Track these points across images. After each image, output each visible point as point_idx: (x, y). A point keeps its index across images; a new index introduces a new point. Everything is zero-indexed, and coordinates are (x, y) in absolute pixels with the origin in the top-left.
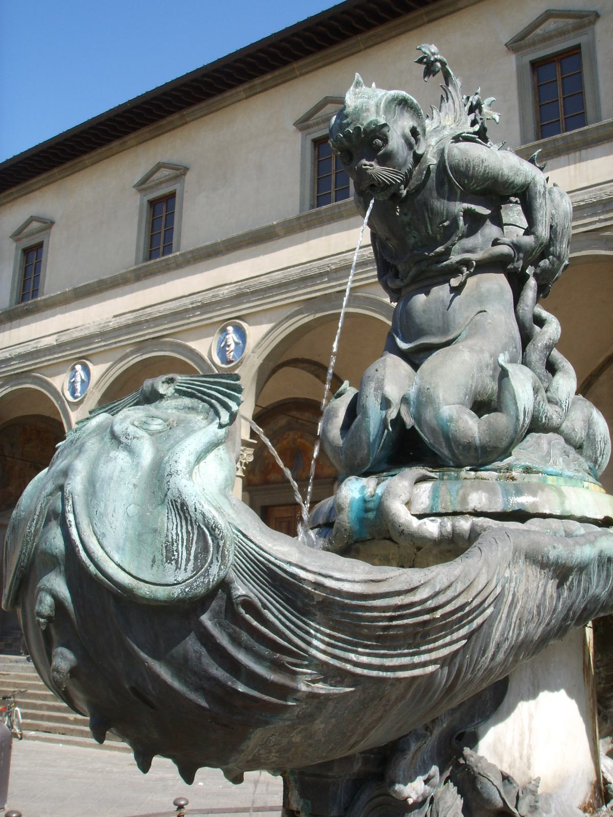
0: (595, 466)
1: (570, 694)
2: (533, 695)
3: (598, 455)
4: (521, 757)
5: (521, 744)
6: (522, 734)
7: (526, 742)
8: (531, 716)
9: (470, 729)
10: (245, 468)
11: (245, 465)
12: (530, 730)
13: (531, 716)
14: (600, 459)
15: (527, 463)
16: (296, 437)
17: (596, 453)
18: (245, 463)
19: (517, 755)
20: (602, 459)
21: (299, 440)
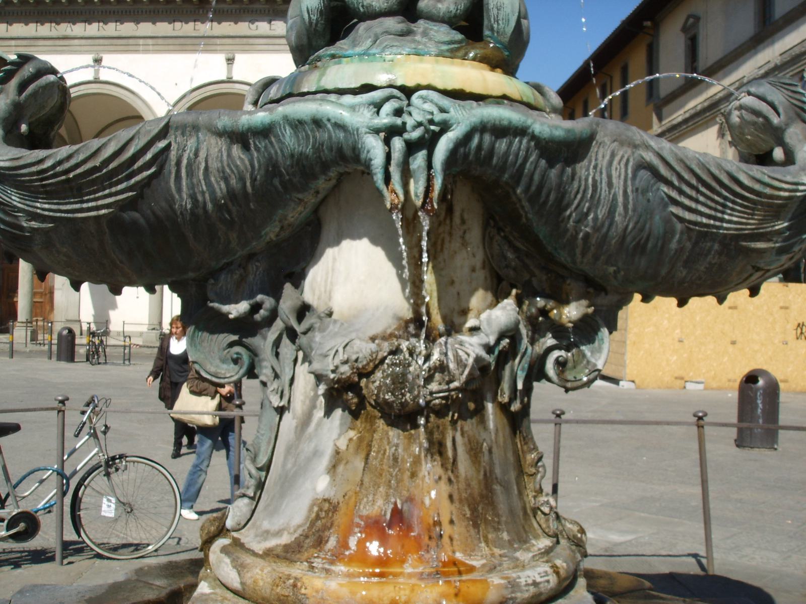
0: (493, 34)
1: (375, 241)
2: (337, 242)
4: (325, 291)
5: (326, 281)
6: (327, 273)
7: (329, 280)
8: (334, 259)
9: (297, 269)
12: (333, 270)
13: (334, 259)
14: (495, 26)
15: (332, 52)
19: (323, 289)
20: (498, 24)
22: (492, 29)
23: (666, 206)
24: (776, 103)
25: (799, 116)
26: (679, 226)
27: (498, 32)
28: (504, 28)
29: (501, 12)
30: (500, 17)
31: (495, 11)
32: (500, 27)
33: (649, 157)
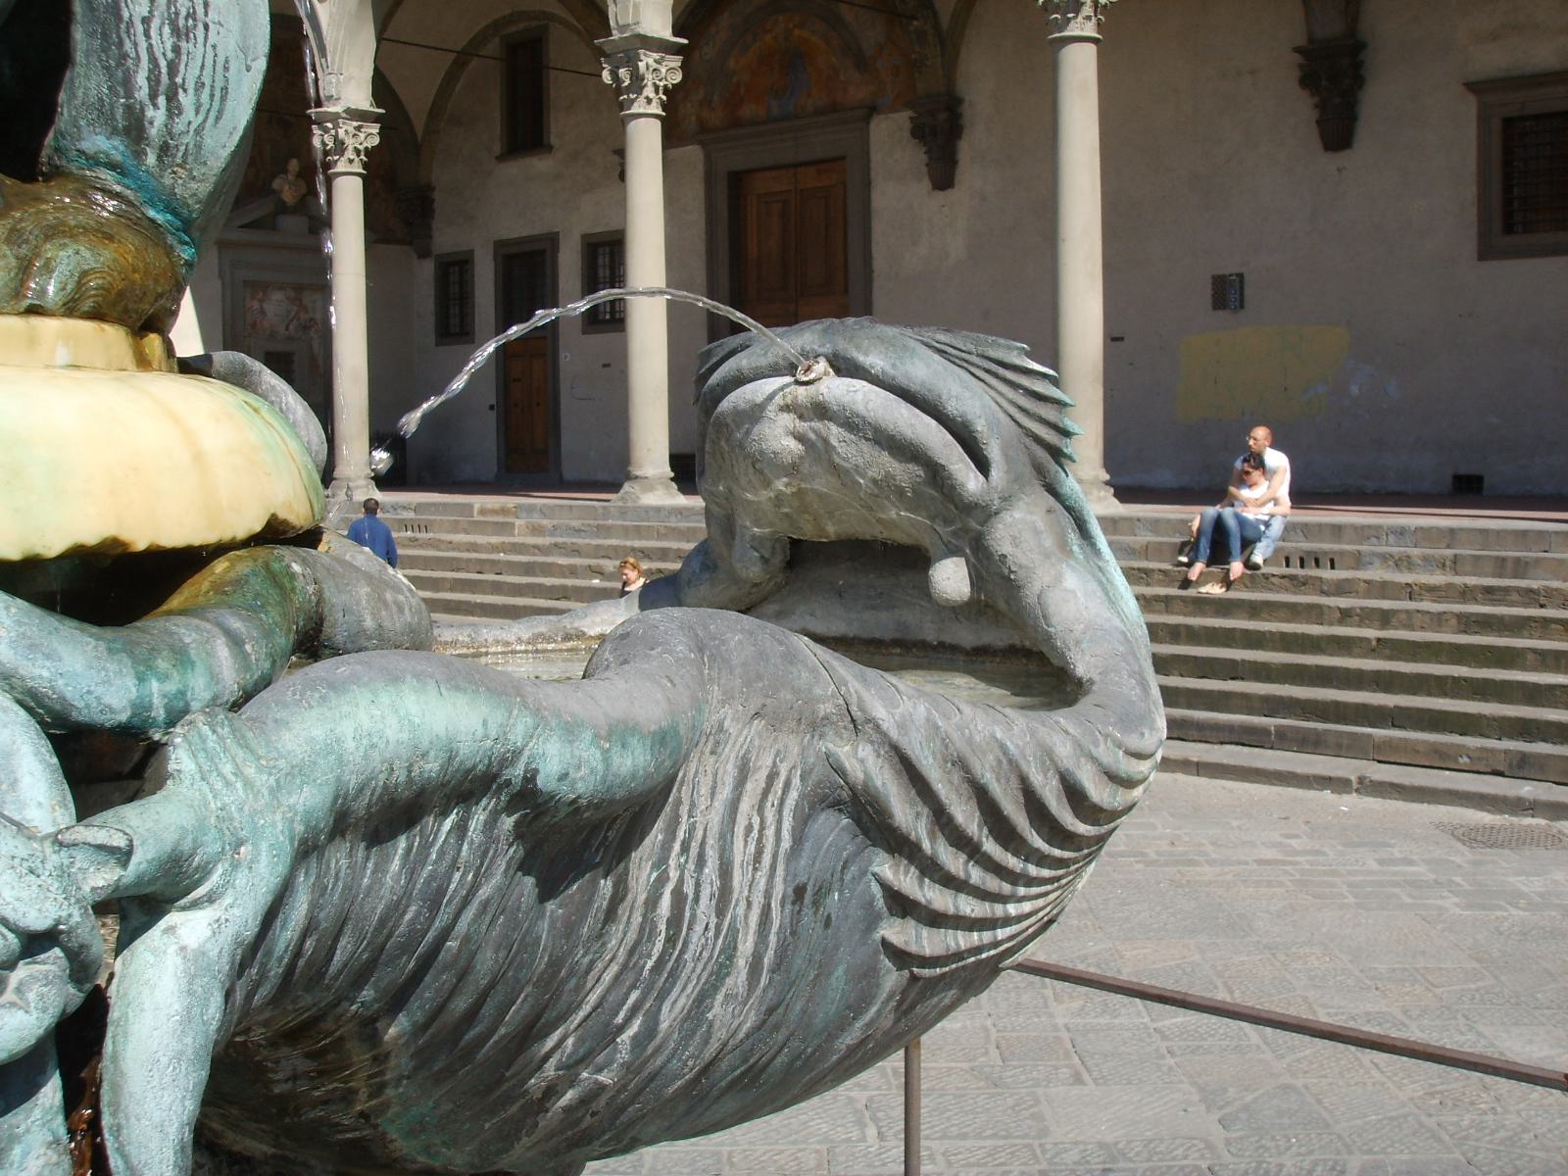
0: (139, 155)
3: (142, 93)
10: (664, 98)
11: (666, 91)
14: (157, 116)
16: (791, 26)
17: (128, 83)
18: (665, 86)
20: (174, 109)
21: (796, 32)
22: (134, 130)
23: (872, 921)
24: (980, 426)
25: (1040, 470)
26: (892, 979)
27: (164, 150)
28: (198, 131)
29: (195, 51)
30: (189, 74)
31: (163, 41)
32: (180, 125)
33: (864, 763)
